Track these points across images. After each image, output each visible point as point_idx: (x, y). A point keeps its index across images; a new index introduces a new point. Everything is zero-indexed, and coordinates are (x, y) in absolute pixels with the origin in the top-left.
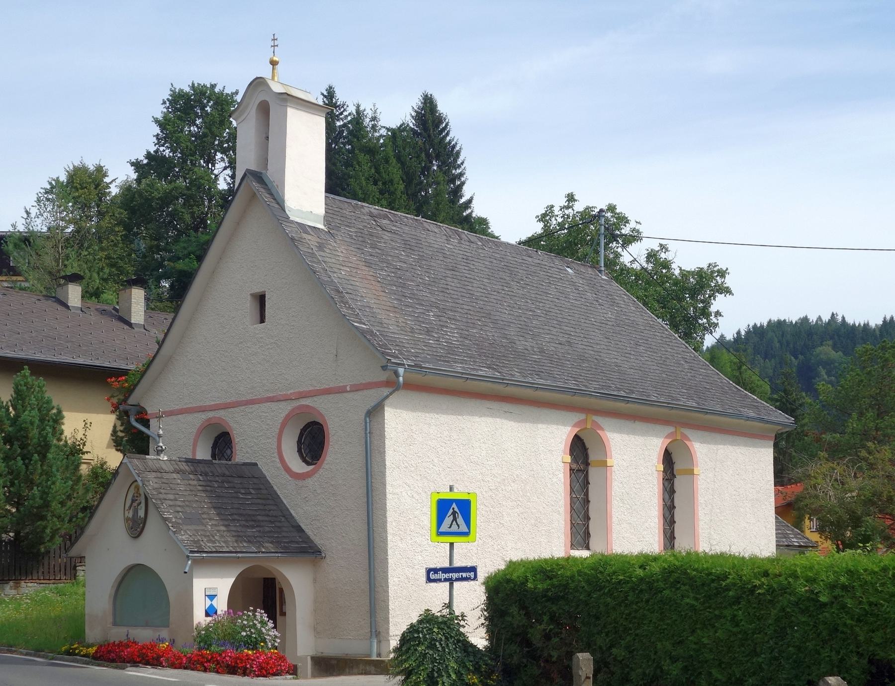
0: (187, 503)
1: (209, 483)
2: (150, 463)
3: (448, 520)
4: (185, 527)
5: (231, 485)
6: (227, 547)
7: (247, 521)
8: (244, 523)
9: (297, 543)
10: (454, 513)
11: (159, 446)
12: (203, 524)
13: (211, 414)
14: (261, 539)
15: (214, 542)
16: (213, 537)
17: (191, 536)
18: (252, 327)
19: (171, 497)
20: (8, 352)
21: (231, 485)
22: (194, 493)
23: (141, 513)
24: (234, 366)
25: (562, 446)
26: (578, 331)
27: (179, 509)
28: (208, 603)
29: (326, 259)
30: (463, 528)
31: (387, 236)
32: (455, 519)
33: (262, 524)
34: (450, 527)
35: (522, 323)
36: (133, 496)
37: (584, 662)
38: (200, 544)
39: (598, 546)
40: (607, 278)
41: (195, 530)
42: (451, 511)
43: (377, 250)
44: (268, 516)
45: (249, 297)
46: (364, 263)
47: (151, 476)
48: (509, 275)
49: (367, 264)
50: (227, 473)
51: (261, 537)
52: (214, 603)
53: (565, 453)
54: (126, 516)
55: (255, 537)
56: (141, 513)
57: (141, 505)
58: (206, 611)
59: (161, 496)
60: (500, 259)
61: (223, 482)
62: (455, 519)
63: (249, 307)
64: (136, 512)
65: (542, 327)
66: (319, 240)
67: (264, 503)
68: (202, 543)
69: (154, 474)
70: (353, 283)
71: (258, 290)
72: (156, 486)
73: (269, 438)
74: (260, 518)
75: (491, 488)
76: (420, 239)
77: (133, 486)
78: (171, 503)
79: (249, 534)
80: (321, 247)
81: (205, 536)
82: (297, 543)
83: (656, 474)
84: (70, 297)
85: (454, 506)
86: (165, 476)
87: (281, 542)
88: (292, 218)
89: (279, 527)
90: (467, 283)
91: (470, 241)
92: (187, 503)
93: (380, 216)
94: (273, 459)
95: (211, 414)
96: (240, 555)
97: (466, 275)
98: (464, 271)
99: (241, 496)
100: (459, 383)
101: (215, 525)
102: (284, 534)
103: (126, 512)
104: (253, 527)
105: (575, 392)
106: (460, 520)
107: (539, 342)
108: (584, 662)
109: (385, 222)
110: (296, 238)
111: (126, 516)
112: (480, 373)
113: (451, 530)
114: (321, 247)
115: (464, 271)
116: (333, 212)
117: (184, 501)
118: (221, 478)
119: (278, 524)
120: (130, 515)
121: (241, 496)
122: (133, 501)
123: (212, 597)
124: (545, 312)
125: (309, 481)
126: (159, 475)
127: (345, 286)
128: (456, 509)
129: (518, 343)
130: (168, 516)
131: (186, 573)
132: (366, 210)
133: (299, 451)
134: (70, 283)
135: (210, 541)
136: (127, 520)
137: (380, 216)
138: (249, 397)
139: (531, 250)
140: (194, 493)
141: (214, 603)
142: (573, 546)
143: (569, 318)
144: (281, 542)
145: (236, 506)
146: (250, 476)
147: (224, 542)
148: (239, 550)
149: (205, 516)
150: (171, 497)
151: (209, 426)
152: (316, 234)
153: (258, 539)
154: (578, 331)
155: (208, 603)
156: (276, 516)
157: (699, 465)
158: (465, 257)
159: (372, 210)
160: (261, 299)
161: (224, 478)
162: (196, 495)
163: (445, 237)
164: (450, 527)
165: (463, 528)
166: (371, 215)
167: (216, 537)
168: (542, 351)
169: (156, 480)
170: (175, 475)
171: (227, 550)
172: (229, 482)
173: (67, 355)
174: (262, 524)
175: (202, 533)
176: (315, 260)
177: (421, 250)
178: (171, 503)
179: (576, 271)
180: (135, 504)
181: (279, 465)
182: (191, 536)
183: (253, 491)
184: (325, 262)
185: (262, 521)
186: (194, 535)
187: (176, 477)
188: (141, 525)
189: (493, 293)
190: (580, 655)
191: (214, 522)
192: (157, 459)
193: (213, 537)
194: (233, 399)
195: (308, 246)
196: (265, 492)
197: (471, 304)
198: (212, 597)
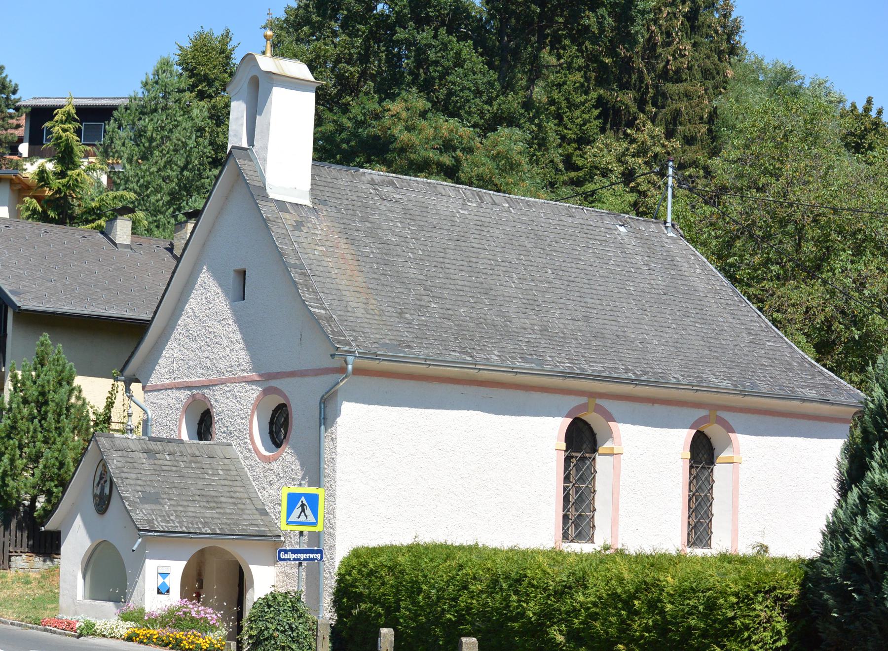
0: (148, 483)
1: (176, 463)
2: (117, 442)
3: (297, 511)
4: (141, 506)
5: (198, 465)
6: (181, 527)
7: (208, 502)
8: (205, 504)
9: (257, 526)
10: (303, 505)
12: (160, 504)
14: (219, 521)
15: (168, 522)
16: (169, 517)
17: (145, 515)
19: (133, 476)
20: (35, 304)
21: (198, 465)
22: (157, 473)
23: (107, 491)
24: (217, 343)
25: (556, 433)
26: (604, 303)
27: (138, 488)
28: (161, 580)
29: (299, 240)
30: (311, 519)
31: (384, 206)
32: (303, 510)
33: (224, 505)
34: (299, 517)
35: (530, 297)
36: (101, 474)
37: (387, 634)
38: (153, 523)
39: (602, 537)
40: (675, 236)
41: (151, 510)
42: (300, 503)
43: (367, 223)
44: (232, 497)
45: (232, 274)
46: (345, 241)
47: (116, 455)
48: (533, 241)
49: (349, 242)
50: (197, 453)
51: (219, 519)
52: (167, 580)
53: (558, 439)
54: (95, 492)
55: (213, 518)
56: (107, 491)
58: (158, 589)
59: (123, 475)
60: (527, 222)
61: (190, 462)
62: (303, 510)
64: (103, 489)
65: (556, 301)
66: (299, 219)
67: (231, 484)
68: (155, 522)
69: (120, 453)
70: (325, 264)
71: (240, 267)
72: (119, 465)
73: (242, 419)
74: (223, 499)
75: (462, 476)
76: (428, 205)
77: (101, 464)
78: (132, 482)
79: (208, 515)
80: (298, 226)
81: (160, 516)
82: (257, 526)
83: (681, 462)
84: (118, 233)
85: (303, 499)
86: (131, 455)
87: (240, 525)
88: (272, 195)
89: (242, 510)
90: (471, 255)
91: (494, 203)
92: (148, 483)
93: (383, 183)
94: (246, 440)
97: (474, 245)
98: (473, 240)
99: (207, 477)
100: (421, 369)
101: (174, 506)
102: (245, 517)
103: (95, 489)
104: (213, 508)
105: (564, 375)
106: (308, 511)
107: (545, 319)
108: (387, 634)
109: (385, 190)
110: (271, 218)
112: (448, 359)
113: (298, 520)
114: (298, 226)
115: (473, 240)
116: (325, 184)
117: (145, 481)
118: (189, 457)
119: (242, 507)
120: (98, 493)
121: (207, 477)
122: (101, 478)
124: (566, 283)
126: (125, 453)
127: (314, 268)
128: (305, 502)
129: (515, 321)
131: (133, 551)
132: (368, 177)
134: (119, 217)
135: (164, 521)
136: (95, 496)
137: (383, 183)
139: (576, 208)
140: (157, 473)
141: (167, 580)
142: (565, 536)
143: (598, 288)
144: (240, 525)
145: (200, 487)
146: (222, 456)
147: (179, 522)
149: (164, 496)
150: (133, 476)
152: (296, 212)
153: (215, 520)
154: (604, 303)
155: (161, 580)
156: (240, 499)
157: (741, 452)
158: (480, 223)
159: (375, 177)
160: (243, 274)
161: (193, 458)
162: (159, 475)
163: (461, 202)
164: (299, 517)
165: (311, 519)
166: (372, 183)
167: (172, 517)
168: (544, 329)
169: (120, 459)
171: (180, 530)
172: (196, 462)
173: (99, 306)
174: (224, 505)
175: (158, 512)
176: (287, 241)
177: (424, 219)
178: (132, 482)
179: (631, 230)
180: (102, 482)
182: (145, 515)
183: (221, 472)
184: (298, 243)
185: (225, 503)
186: (149, 514)
187: (142, 456)
189: (503, 264)
190: (384, 631)
191: (172, 502)
192: (126, 438)
193: (169, 517)
195: (282, 225)
196: (235, 473)
197: (469, 279)
198: (164, 575)
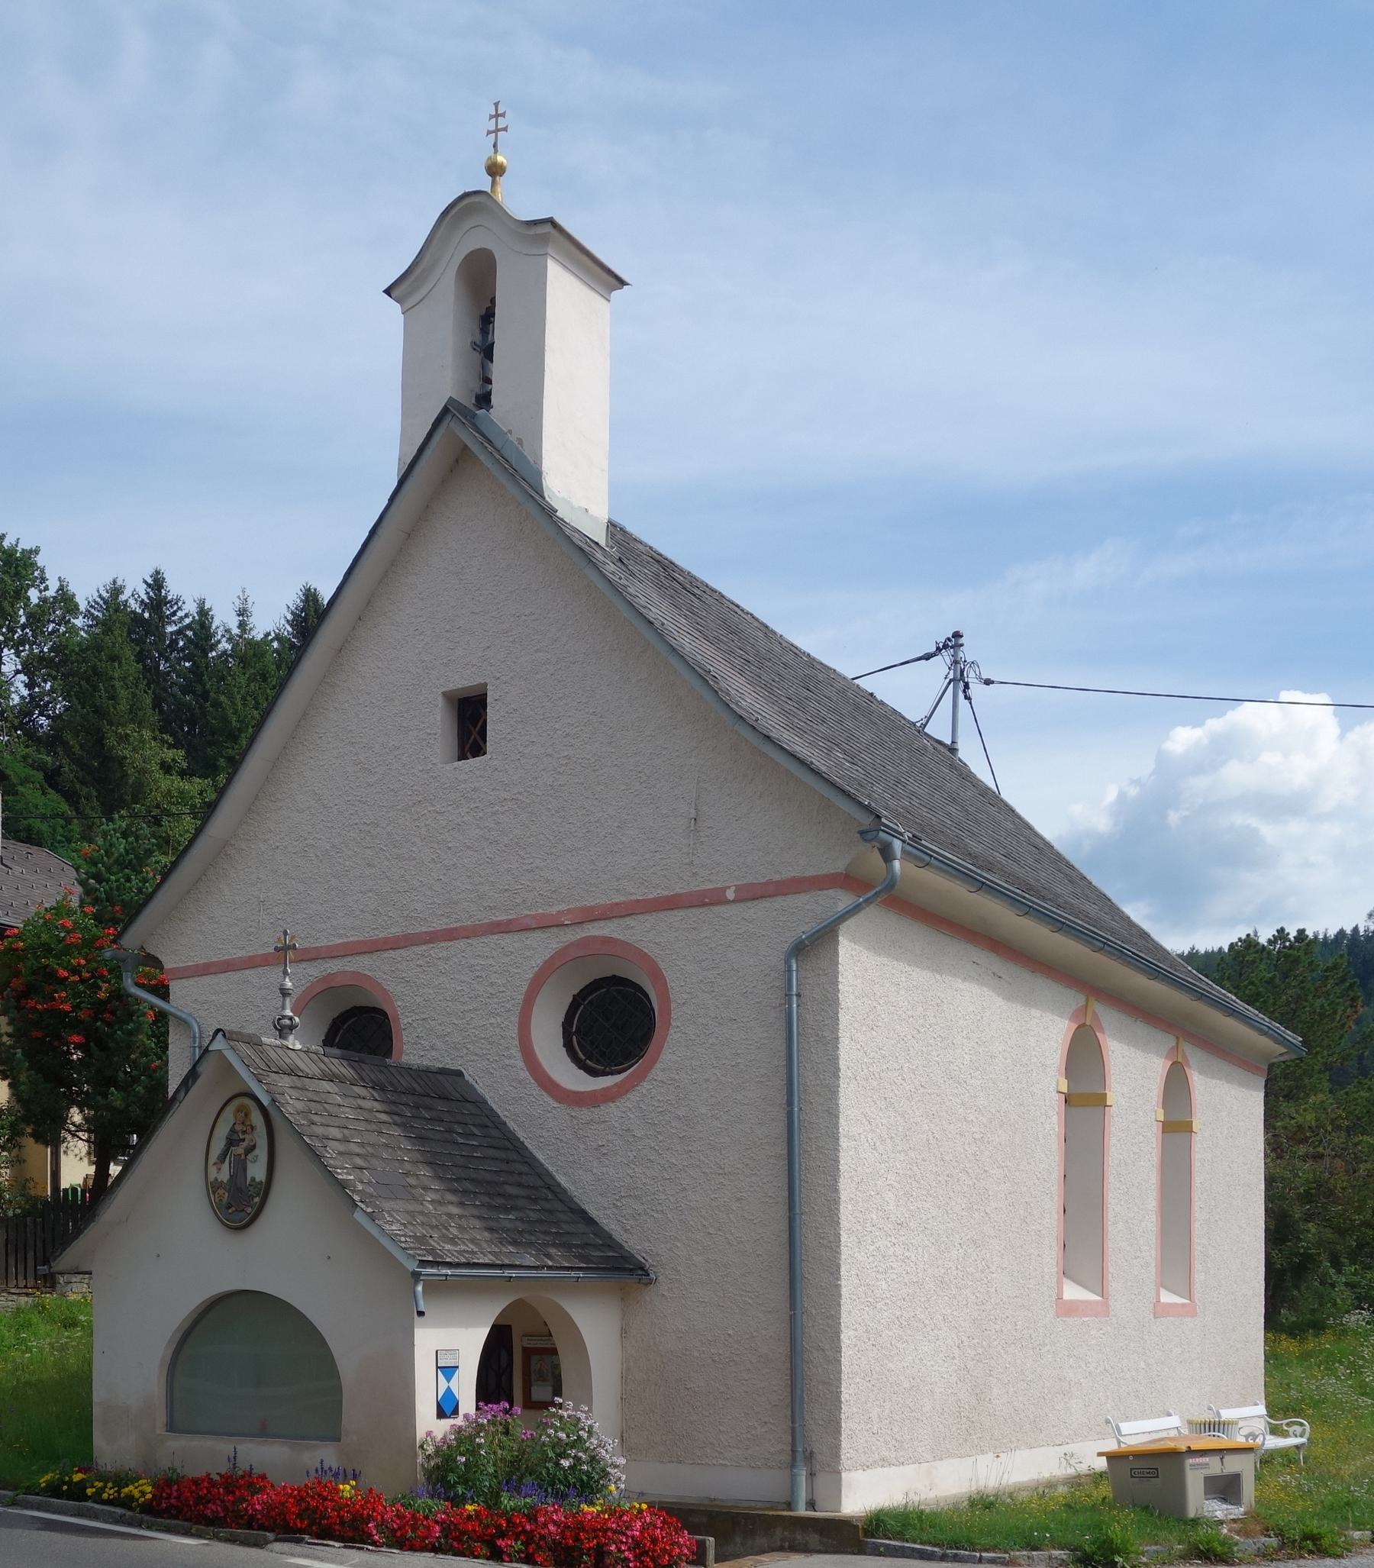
0: (370, 1149)
8: (486, 1199)
11: (284, 1017)
12: (415, 1199)
13: (333, 966)
18: (449, 767)
27: (360, 1162)
36: (233, 1131)
45: (440, 699)
51: (530, 1233)
52: (454, 1385)
54: (211, 1178)
56: (257, 1171)
57: (257, 1151)
63: (440, 724)
71: (463, 680)
72: (300, 1106)
77: (229, 1112)
95: (333, 966)
96: (514, 1273)
111: (211, 1178)
117: (362, 1145)
120: (224, 1175)
122: (231, 1142)
123: (449, 1371)
125: (613, 1111)
130: (345, 1177)
133: (568, 1045)
136: (213, 1187)
138: (440, 924)
141: (454, 1385)
148: (507, 1262)
151: (324, 992)
169: (295, 1094)
170: (326, 1086)
181: (525, 1074)
188: (257, 1200)
194: (395, 931)
198: (449, 1371)
